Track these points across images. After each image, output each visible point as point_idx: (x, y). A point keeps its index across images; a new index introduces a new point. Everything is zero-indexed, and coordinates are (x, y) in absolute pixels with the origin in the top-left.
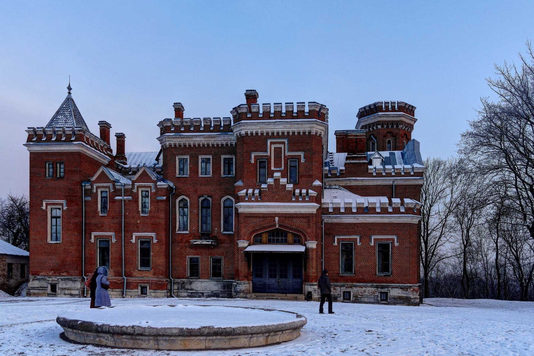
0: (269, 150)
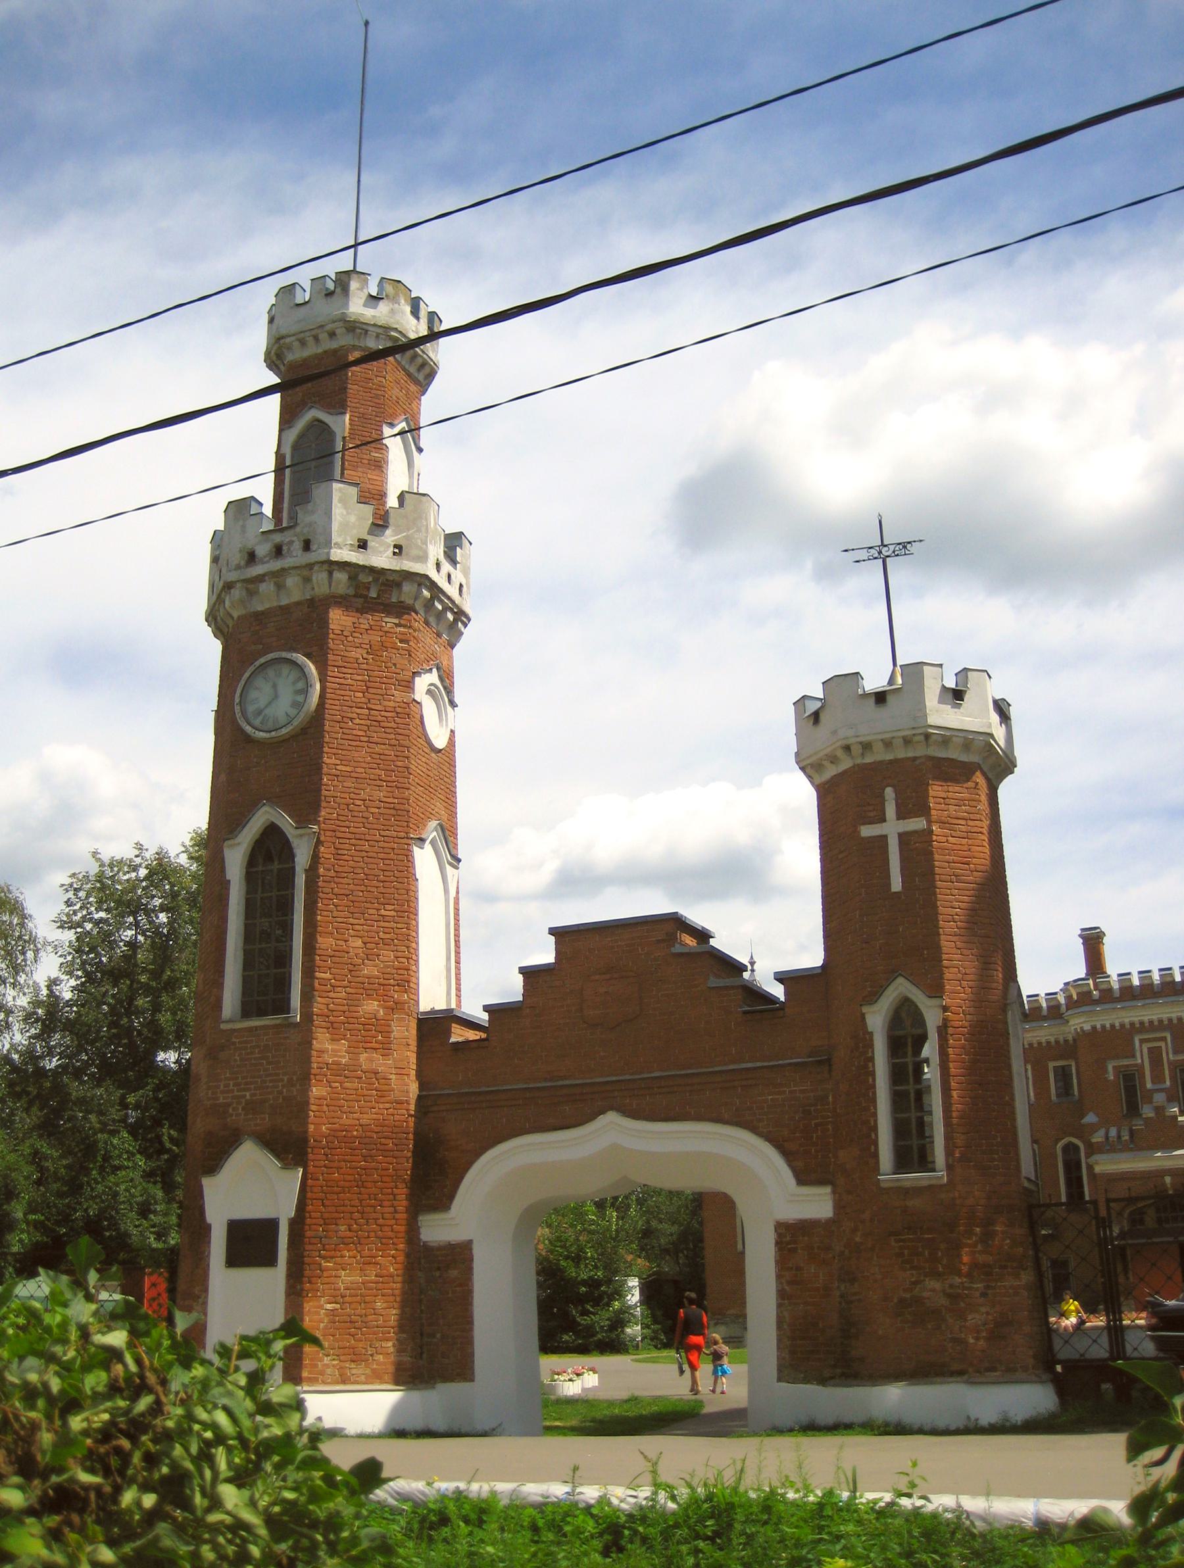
0: (1138, 1054)
